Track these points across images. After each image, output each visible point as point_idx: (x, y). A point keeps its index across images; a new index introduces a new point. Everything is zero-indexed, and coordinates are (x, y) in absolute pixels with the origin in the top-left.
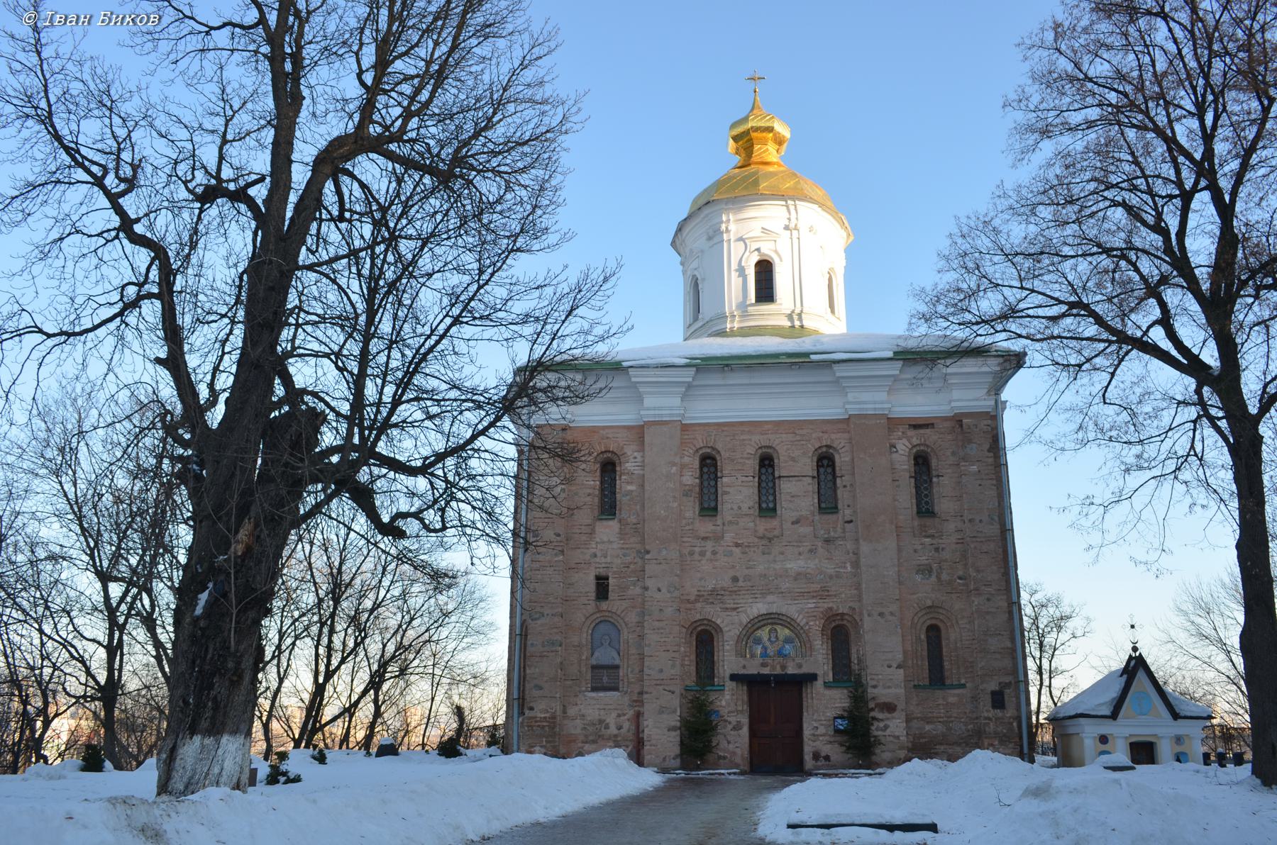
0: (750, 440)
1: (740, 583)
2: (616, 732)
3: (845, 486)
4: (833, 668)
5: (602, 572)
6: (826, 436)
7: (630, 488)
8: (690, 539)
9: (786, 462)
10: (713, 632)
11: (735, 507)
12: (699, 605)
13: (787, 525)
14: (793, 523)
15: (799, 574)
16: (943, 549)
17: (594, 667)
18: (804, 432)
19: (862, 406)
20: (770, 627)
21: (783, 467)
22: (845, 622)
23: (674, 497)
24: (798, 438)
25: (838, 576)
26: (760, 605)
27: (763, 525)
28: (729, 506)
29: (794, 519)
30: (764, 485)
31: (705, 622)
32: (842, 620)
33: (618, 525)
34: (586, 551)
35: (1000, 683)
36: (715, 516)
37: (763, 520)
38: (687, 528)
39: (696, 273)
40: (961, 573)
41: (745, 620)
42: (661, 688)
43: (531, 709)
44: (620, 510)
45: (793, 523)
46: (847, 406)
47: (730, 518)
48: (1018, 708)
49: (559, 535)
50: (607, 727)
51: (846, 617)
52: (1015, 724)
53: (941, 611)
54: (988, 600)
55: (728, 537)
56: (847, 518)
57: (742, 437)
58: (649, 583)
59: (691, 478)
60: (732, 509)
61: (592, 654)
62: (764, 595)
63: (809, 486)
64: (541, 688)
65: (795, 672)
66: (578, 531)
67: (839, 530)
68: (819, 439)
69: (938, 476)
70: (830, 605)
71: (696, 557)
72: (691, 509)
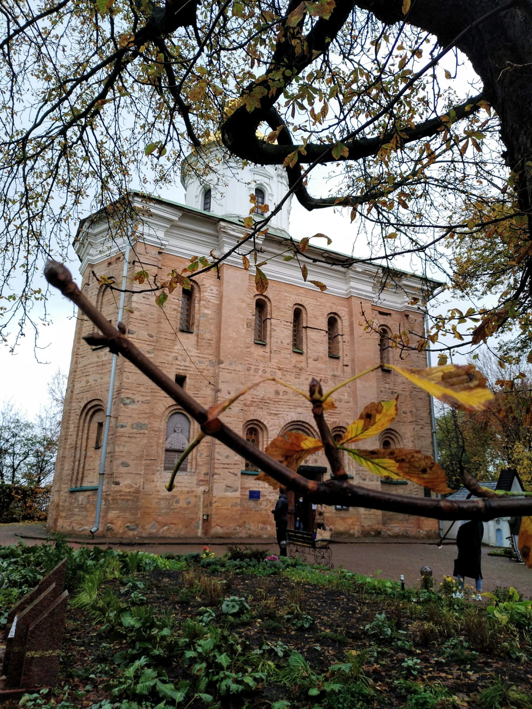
1: (280, 397)
2: (185, 506)
3: (344, 342)
5: (182, 373)
6: (334, 306)
7: (206, 311)
8: (248, 359)
9: (311, 318)
10: (259, 429)
11: (279, 342)
12: (252, 409)
13: (310, 361)
17: (167, 450)
18: (322, 300)
21: (307, 320)
24: (319, 304)
27: (296, 358)
28: (275, 340)
31: (256, 422)
32: (340, 431)
33: (196, 338)
34: (169, 353)
36: (265, 345)
37: (295, 354)
40: (404, 410)
41: (283, 424)
42: (227, 470)
43: (117, 484)
44: (198, 326)
46: (351, 290)
47: (275, 349)
49: (151, 336)
50: (177, 502)
53: (393, 432)
54: (422, 428)
55: (274, 362)
56: (346, 363)
57: (285, 294)
58: (221, 386)
61: (166, 439)
62: (296, 407)
63: (323, 337)
64: (128, 466)
66: (165, 337)
67: (340, 370)
68: (331, 307)
70: (335, 420)
71: (252, 372)
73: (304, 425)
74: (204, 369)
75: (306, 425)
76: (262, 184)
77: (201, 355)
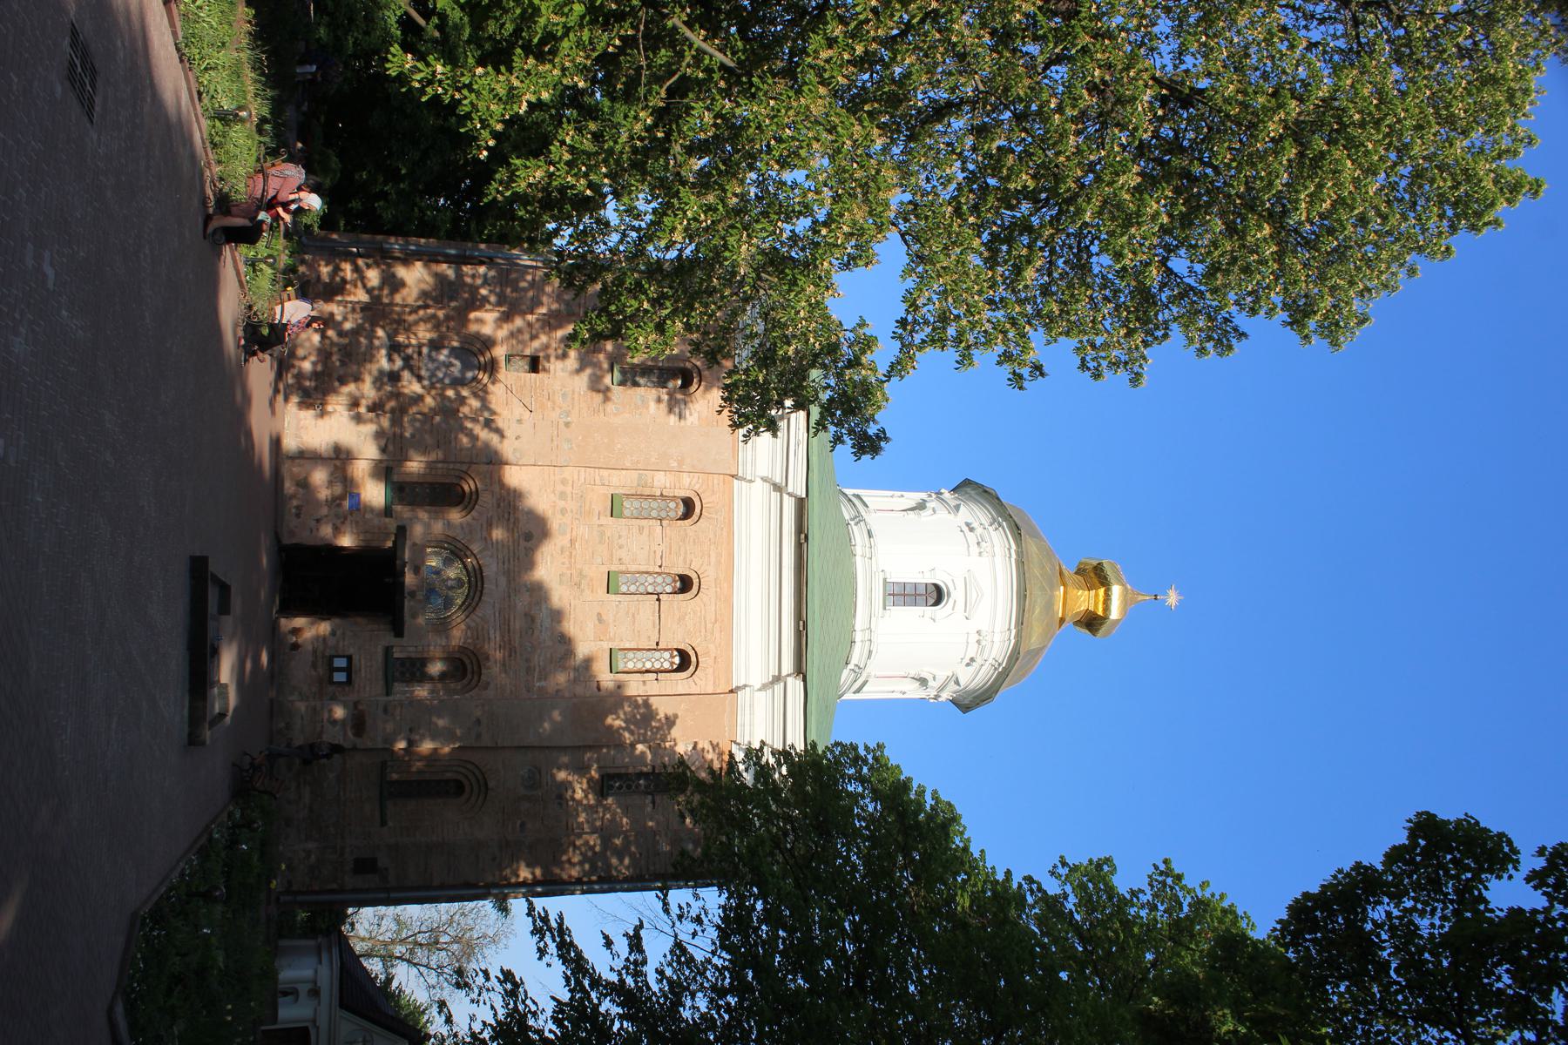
0: (709, 564)
1: (522, 542)
4: (409, 658)
11: (622, 541)
14: (599, 615)
15: (533, 620)
16: (560, 804)
19: (747, 712)
20: (465, 579)
22: (469, 676)
23: (638, 462)
25: (529, 670)
26: (494, 567)
29: (604, 617)
30: (650, 579)
32: (473, 673)
35: (386, 869)
38: (597, 478)
39: (928, 512)
45: (599, 615)
47: (608, 534)
48: (355, 891)
51: (476, 678)
52: (335, 886)
54: (494, 859)
57: (713, 555)
59: (661, 482)
60: (620, 537)
65: (406, 610)
68: (707, 654)
69: (653, 802)
71: (560, 488)
72: (622, 481)
73: (478, 594)
74: (554, 402)
75: (476, 598)
76: (949, 595)
77: (576, 396)
